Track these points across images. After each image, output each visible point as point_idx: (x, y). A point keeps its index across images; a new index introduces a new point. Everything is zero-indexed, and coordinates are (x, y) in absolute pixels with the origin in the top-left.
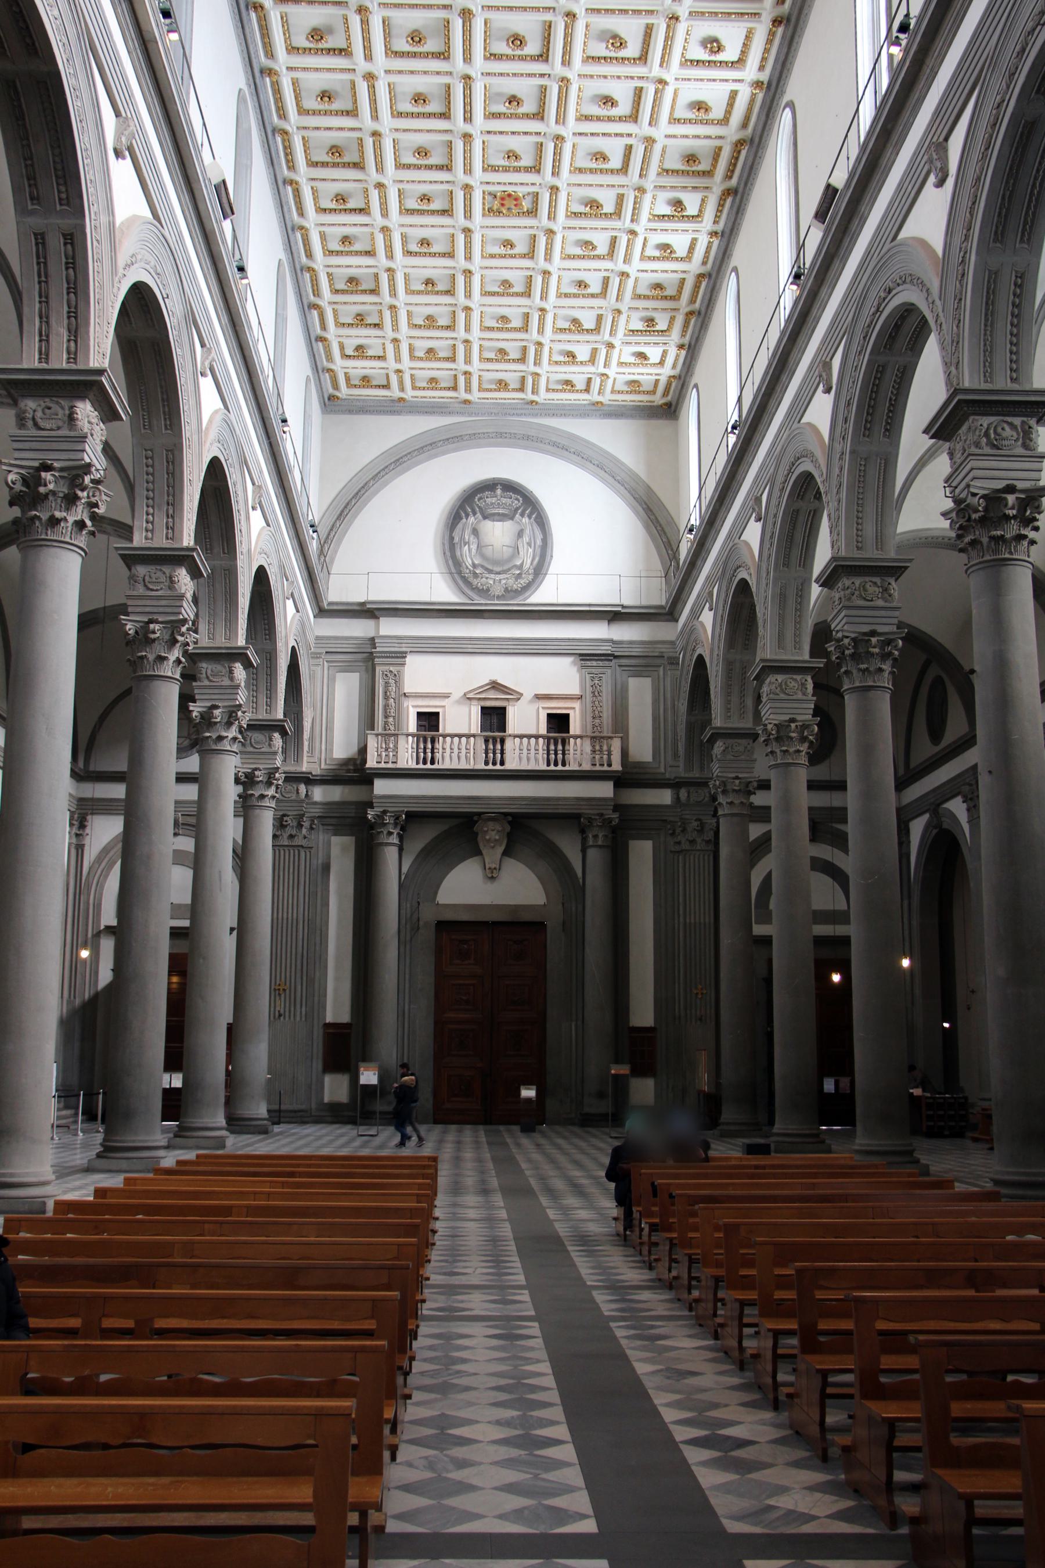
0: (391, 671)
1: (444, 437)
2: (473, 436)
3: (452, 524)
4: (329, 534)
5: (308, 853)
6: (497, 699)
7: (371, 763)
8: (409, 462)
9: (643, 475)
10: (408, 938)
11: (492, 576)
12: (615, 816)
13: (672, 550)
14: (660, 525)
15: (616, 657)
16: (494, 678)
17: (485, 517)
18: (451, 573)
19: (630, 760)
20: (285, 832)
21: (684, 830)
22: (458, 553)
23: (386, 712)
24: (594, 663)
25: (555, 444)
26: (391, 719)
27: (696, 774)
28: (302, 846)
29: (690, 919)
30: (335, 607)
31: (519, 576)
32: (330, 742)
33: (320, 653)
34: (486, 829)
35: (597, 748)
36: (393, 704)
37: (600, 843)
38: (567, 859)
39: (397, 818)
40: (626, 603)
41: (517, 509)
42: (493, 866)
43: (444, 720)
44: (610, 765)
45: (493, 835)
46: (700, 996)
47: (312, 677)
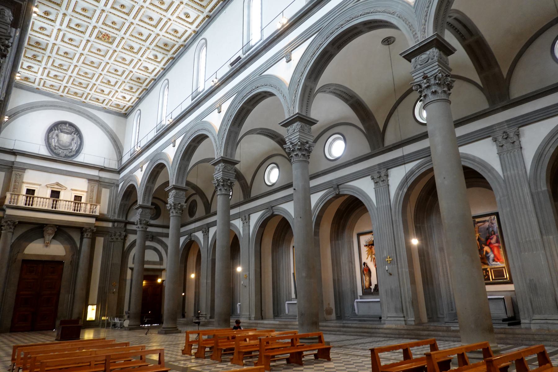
3: (50, 131)
7: (7, 202)
11: (62, 150)
17: (61, 132)
18: (46, 146)
22: (50, 141)
41: (73, 132)
42: (48, 242)
45: (50, 232)
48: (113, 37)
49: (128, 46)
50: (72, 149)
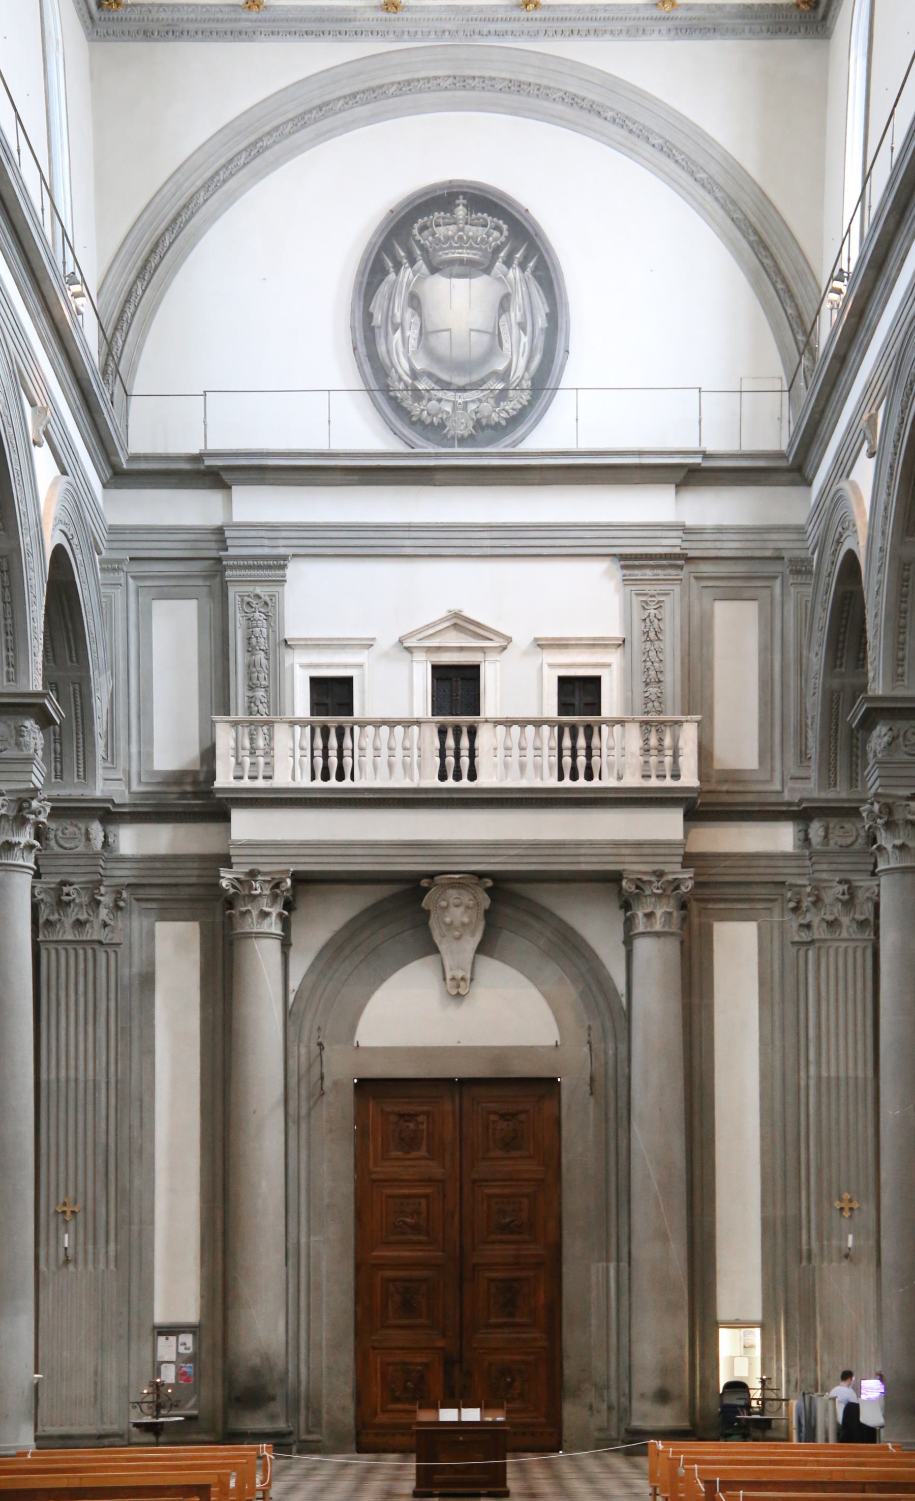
0: (258, 597)
1: (347, 91)
2: (407, 86)
3: (369, 283)
4: (123, 311)
5: (112, 956)
6: (461, 649)
7: (224, 779)
8: (276, 148)
9: (752, 168)
10: (304, 1111)
11: (450, 395)
12: (688, 874)
13: (805, 332)
14: (784, 280)
15: (689, 559)
16: (455, 607)
17: (434, 270)
18: (369, 390)
19: (717, 766)
20: (66, 916)
21: (818, 901)
22: (382, 349)
23: (250, 679)
24: (649, 574)
25: (574, 101)
26: (260, 693)
27: (840, 793)
28: (100, 942)
29: (829, 1070)
30: (143, 466)
31: (502, 396)
32: (146, 739)
33: (120, 561)
34: (444, 904)
35: (653, 741)
36: (264, 662)
37: (658, 927)
38: (597, 957)
39: (277, 886)
40: (710, 446)
41: (497, 250)
42: (459, 974)
43: (363, 691)
44: (676, 776)
45: (457, 915)
46: (846, 1214)
47: (106, 612)
50: (508, 370)
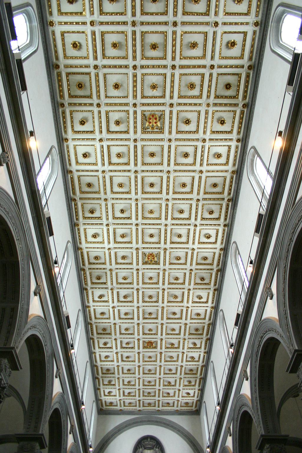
17: (145, 448)
48: (155, 342)
49: (169, 344)
